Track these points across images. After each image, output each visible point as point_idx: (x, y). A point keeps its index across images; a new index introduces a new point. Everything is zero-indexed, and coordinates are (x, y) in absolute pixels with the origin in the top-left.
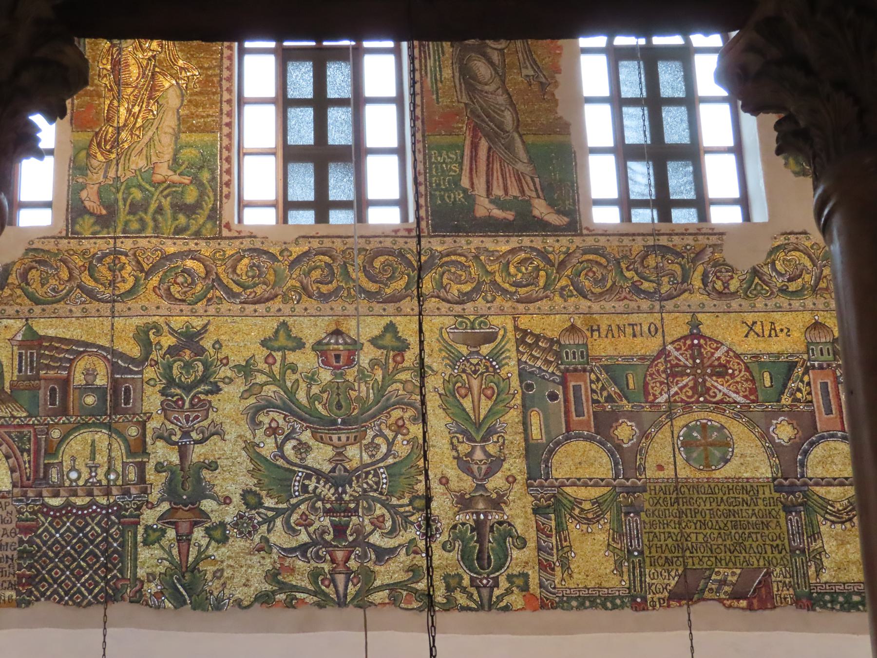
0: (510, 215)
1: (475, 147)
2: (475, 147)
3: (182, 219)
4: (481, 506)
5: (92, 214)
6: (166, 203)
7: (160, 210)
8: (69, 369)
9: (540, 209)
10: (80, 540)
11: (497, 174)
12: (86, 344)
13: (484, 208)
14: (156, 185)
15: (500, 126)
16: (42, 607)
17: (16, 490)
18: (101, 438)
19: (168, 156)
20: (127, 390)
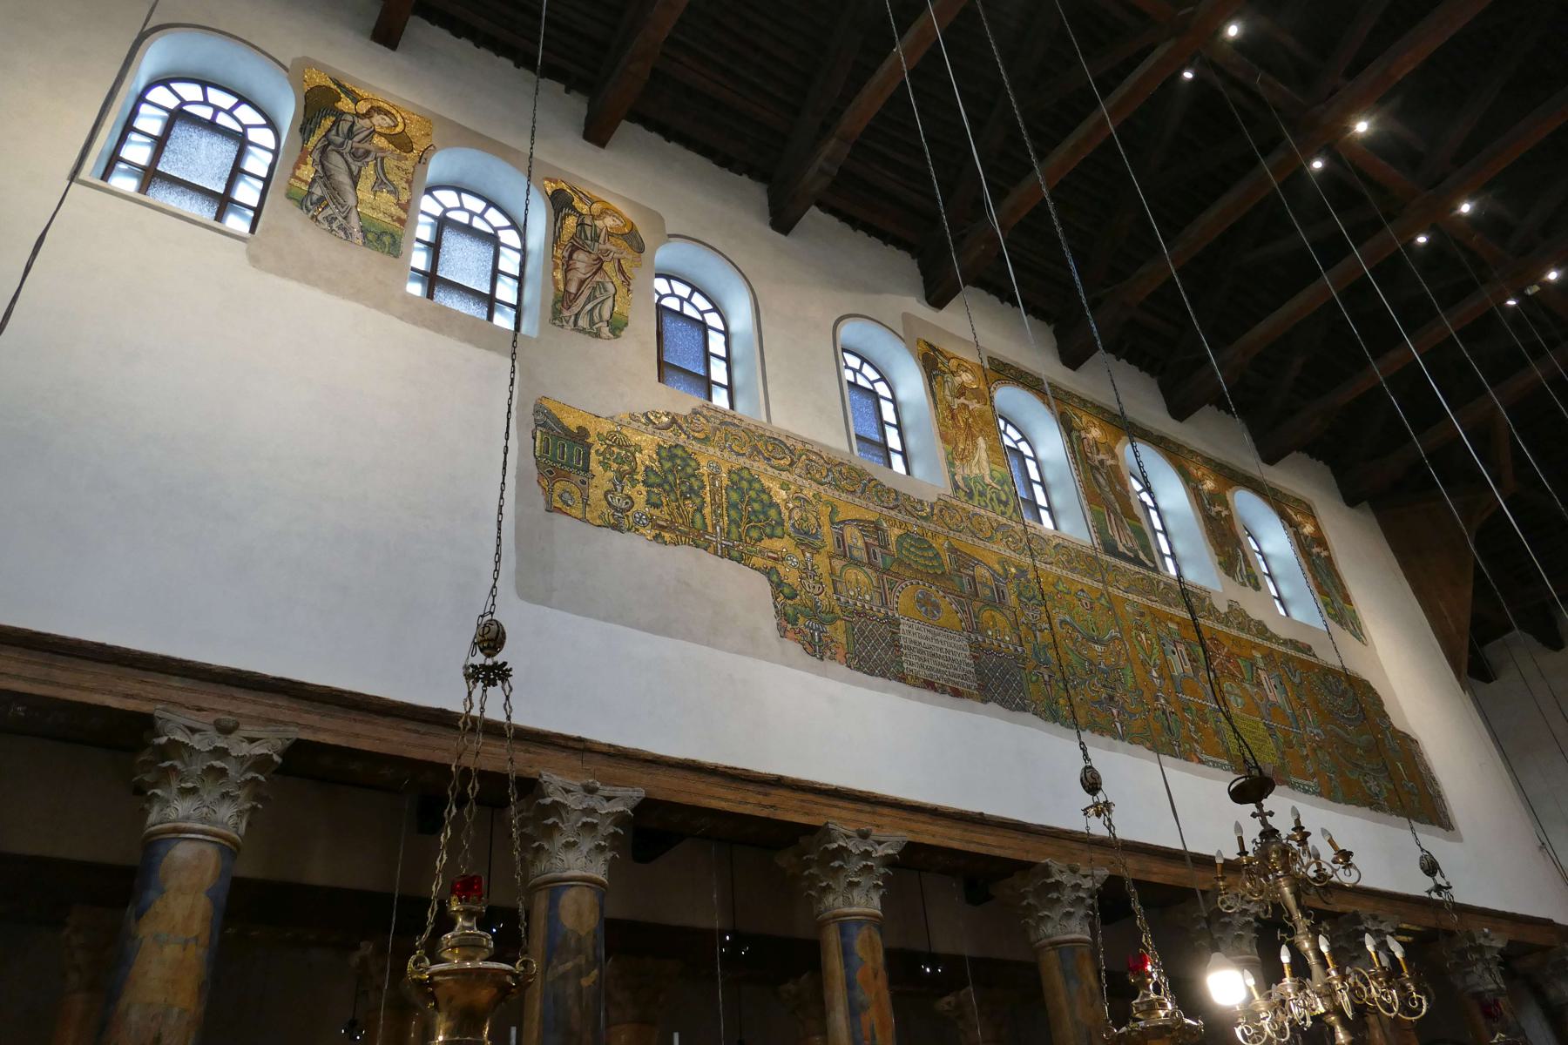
0: (1132, 555)
1: (1109, 516)
2: (1109, 516)
3: (1002, 508)
4: (1163, 701)
5: (962, 490)
6: (994, 495)
7: (991, 499)
8: (973, 571)
9: (1142, 556)
10: (1001, 671)
11: (1121, 533)
12: (979, 561)
13: (1121, 548)
14: (988, 485)
15: (1116, 509)
16: (992, 706)
17: (965, 633)
18: (998, 616)
19: (988, 472)
20: (1002, 591)
